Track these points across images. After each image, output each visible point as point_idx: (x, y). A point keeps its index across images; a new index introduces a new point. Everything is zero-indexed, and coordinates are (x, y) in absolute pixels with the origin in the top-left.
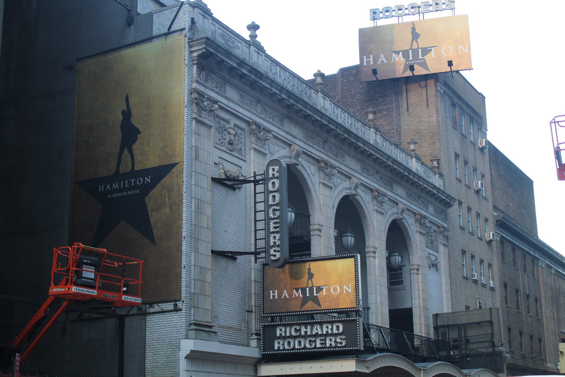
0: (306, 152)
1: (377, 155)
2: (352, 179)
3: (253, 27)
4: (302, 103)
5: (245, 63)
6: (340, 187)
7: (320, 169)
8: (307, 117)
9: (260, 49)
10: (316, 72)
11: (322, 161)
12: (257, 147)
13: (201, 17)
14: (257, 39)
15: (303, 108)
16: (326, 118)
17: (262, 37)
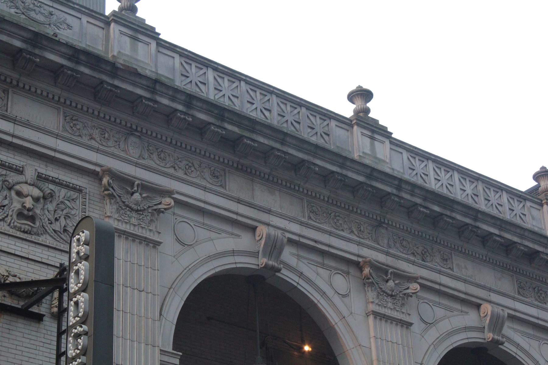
0: (296, 238)
1: (527, 243)
2: (482, 307)
3: (362, 95)
4: (530, 235)
5: (162, 84)
6: (445, 326)
7: (367, 283)
8: (297, 166)
9: (377, 131)
10: (538, 169)
11: (365, 262)
12: (382, 311)
13: (128, 40)
14: (370, 115)
15: (278, 146)
16: (459, 208)
17: (377, 111)
